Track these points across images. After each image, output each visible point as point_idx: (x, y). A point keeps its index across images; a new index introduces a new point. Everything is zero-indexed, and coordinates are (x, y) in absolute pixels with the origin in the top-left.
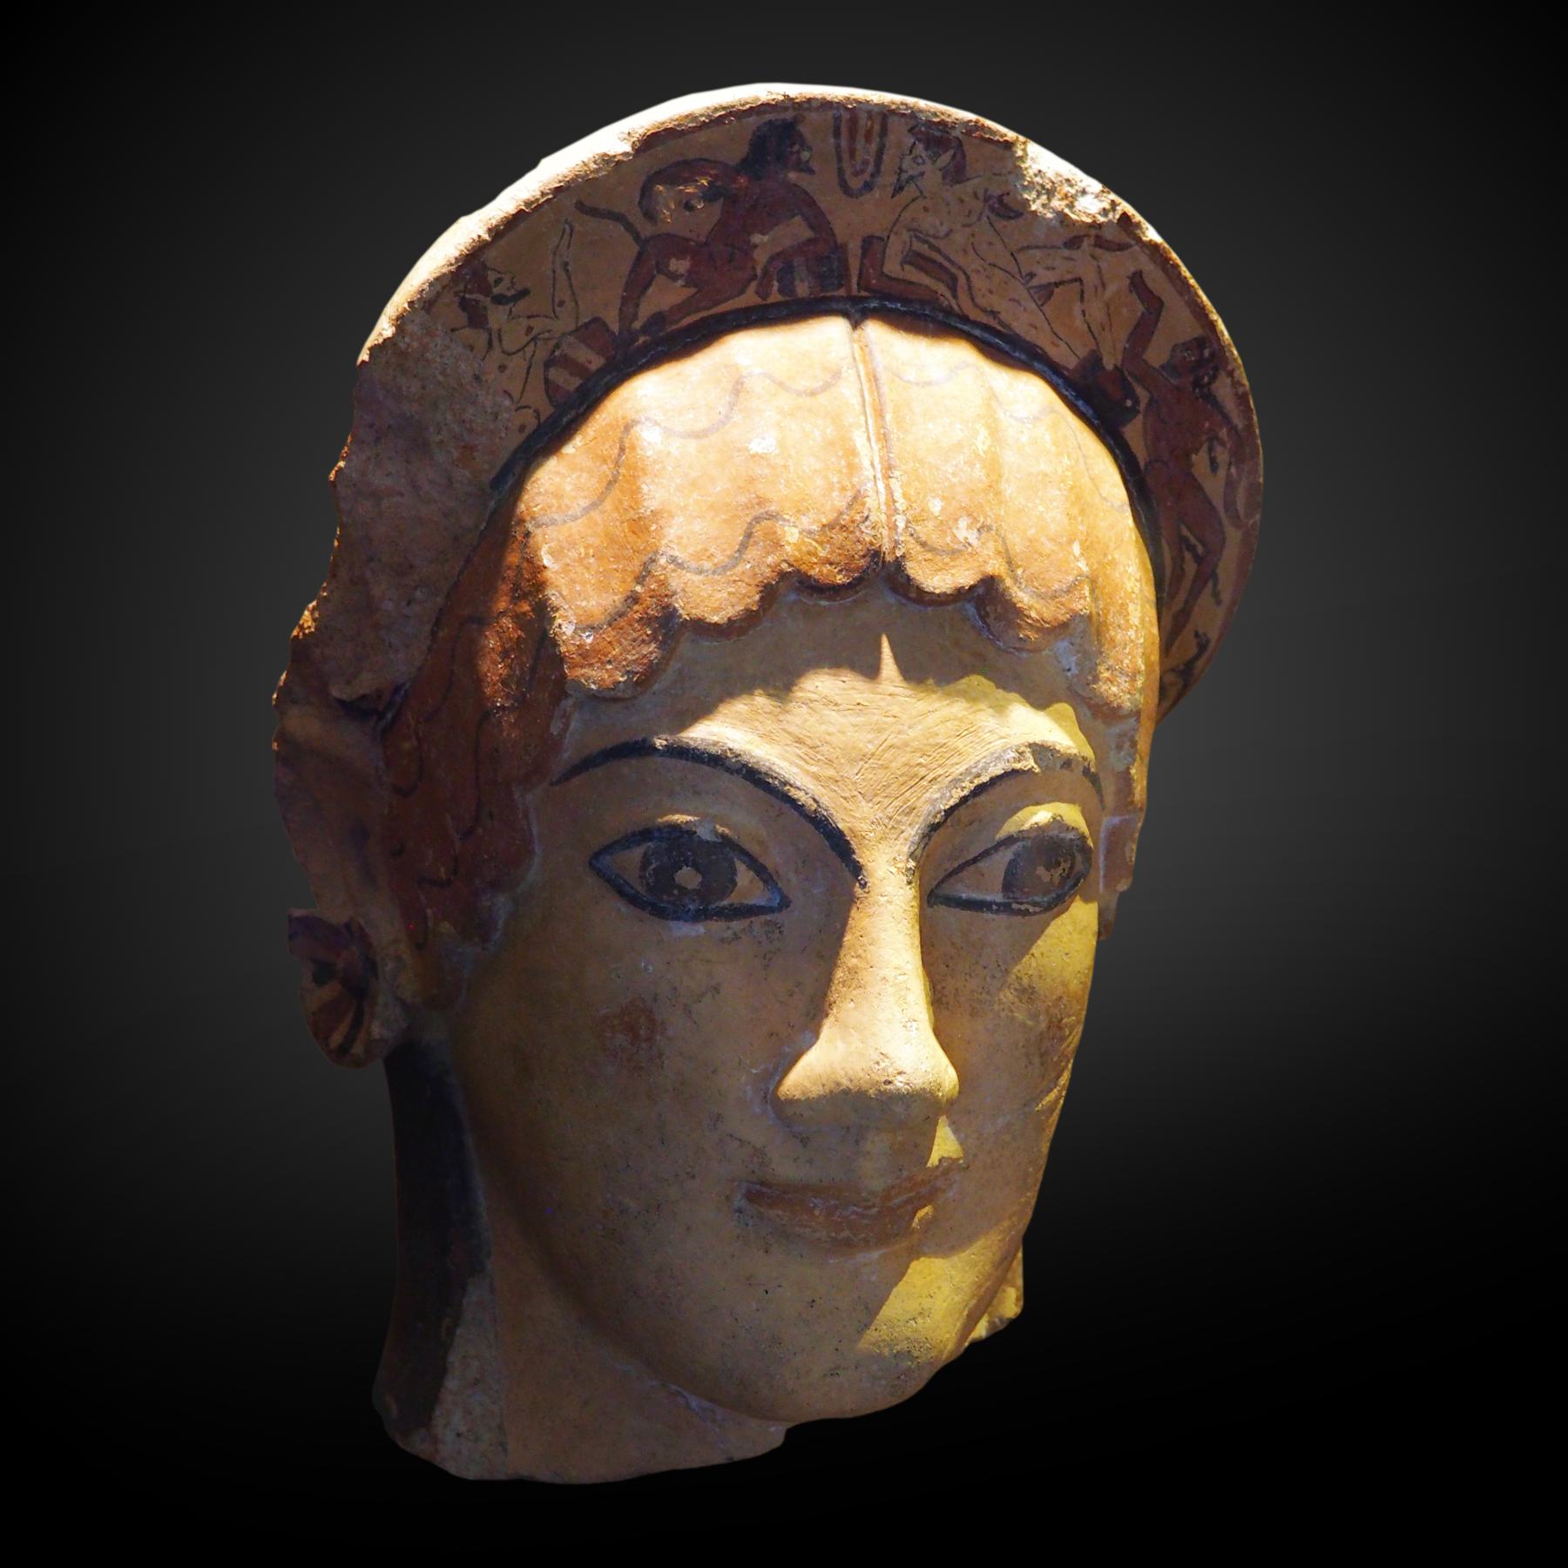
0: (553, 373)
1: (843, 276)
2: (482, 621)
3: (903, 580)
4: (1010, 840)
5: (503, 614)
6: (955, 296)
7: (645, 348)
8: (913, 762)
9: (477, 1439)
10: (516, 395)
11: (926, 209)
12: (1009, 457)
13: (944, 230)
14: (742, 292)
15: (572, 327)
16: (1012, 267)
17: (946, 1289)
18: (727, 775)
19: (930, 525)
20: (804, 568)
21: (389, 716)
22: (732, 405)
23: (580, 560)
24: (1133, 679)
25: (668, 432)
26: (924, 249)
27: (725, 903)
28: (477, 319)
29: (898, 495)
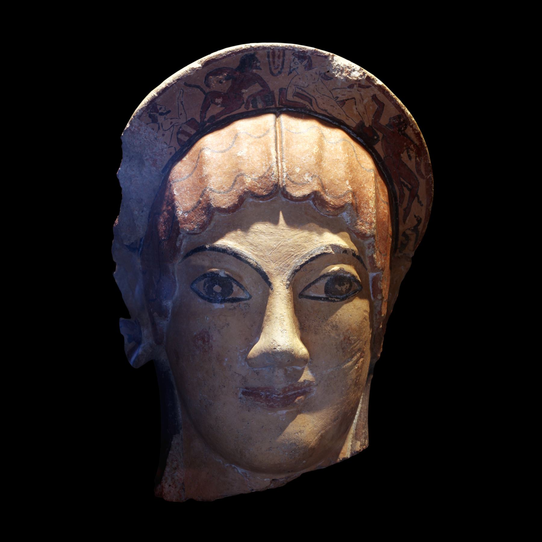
0: (180, 136)
1: (274, 101)
2: (159, 214)
3: (285, 193)
4: (324, 276)
5: (164, 211)
6: (312, 106)
7: (209, 127)
8: (289, 250)
9: (176, 487)
10: (168, 144)
11: (300, 79)
12: (326, 154)
13: (306, 85)
14: (240, 108)
15: (185, 121)
16: (331, 96)
17: (311, 425)
18: (228, 256)
19: (295, 176)
20: (252, 190)
21: (141, 249)
22: (233, 142)
23: (185, 192)
24: (371, 224)
25: (213, 152)
26: (300, 91)
27: (230, 297)
28: (154, 120)
29: (284, 167)
